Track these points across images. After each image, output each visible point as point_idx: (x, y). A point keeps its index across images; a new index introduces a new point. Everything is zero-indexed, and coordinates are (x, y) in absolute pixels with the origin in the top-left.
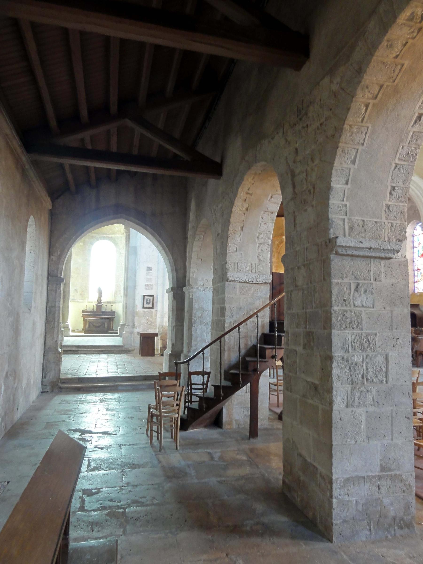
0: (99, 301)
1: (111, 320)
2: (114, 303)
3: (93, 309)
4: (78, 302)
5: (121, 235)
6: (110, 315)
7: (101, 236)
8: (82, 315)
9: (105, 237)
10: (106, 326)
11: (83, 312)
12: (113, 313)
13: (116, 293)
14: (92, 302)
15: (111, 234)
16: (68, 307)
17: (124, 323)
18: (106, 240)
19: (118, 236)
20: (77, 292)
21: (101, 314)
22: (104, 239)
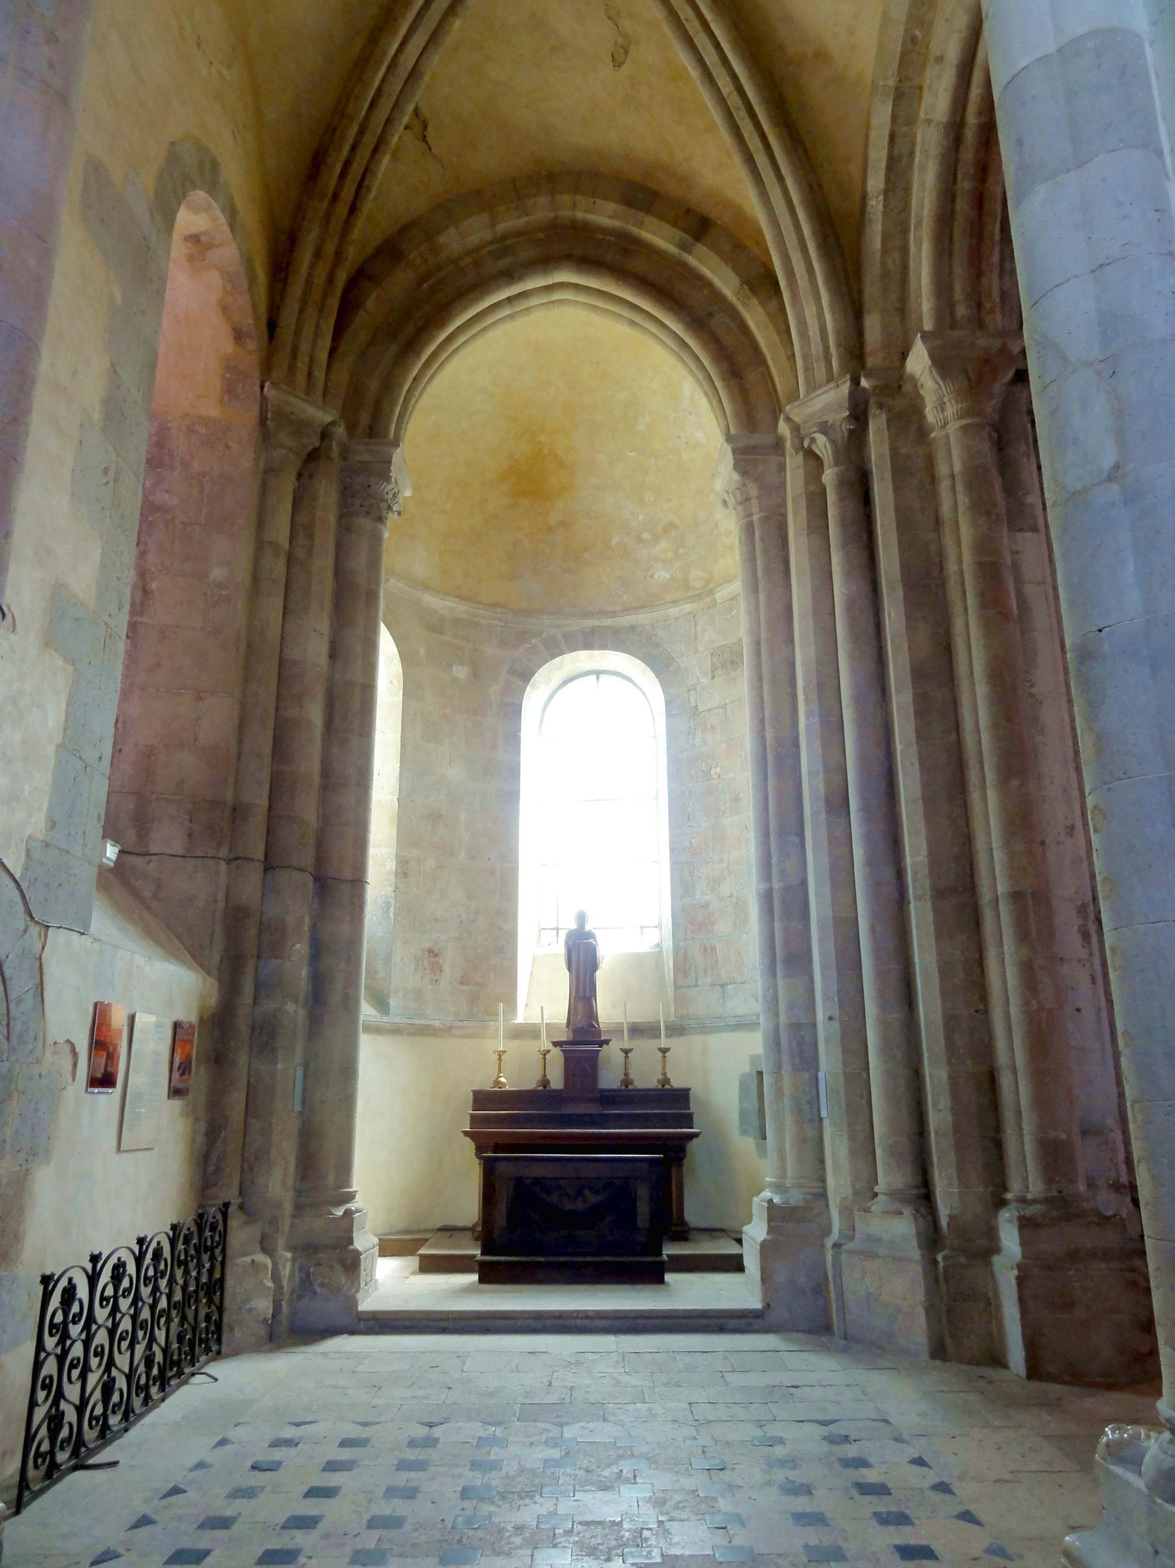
1: (674, 1152)
2: (676, 1030)
3: (545, 1082)
4: (448, 1030)
5: (688, 607)
6: (663, 1121)
7: (575, 625)
8: (474, 1120)
9: (593, 630)
10: (643, 1209)
11: (482, 1099)
12: (674, 1103)
13: (683, 966)
14: (530, 1032)
15: (628, 610)
16: (348, 1072)
17: (796, 1198)
18: (603, 647)
19: (673, 611)
20: (437, 969)
21: (594, 1109)
22: (588, 646)
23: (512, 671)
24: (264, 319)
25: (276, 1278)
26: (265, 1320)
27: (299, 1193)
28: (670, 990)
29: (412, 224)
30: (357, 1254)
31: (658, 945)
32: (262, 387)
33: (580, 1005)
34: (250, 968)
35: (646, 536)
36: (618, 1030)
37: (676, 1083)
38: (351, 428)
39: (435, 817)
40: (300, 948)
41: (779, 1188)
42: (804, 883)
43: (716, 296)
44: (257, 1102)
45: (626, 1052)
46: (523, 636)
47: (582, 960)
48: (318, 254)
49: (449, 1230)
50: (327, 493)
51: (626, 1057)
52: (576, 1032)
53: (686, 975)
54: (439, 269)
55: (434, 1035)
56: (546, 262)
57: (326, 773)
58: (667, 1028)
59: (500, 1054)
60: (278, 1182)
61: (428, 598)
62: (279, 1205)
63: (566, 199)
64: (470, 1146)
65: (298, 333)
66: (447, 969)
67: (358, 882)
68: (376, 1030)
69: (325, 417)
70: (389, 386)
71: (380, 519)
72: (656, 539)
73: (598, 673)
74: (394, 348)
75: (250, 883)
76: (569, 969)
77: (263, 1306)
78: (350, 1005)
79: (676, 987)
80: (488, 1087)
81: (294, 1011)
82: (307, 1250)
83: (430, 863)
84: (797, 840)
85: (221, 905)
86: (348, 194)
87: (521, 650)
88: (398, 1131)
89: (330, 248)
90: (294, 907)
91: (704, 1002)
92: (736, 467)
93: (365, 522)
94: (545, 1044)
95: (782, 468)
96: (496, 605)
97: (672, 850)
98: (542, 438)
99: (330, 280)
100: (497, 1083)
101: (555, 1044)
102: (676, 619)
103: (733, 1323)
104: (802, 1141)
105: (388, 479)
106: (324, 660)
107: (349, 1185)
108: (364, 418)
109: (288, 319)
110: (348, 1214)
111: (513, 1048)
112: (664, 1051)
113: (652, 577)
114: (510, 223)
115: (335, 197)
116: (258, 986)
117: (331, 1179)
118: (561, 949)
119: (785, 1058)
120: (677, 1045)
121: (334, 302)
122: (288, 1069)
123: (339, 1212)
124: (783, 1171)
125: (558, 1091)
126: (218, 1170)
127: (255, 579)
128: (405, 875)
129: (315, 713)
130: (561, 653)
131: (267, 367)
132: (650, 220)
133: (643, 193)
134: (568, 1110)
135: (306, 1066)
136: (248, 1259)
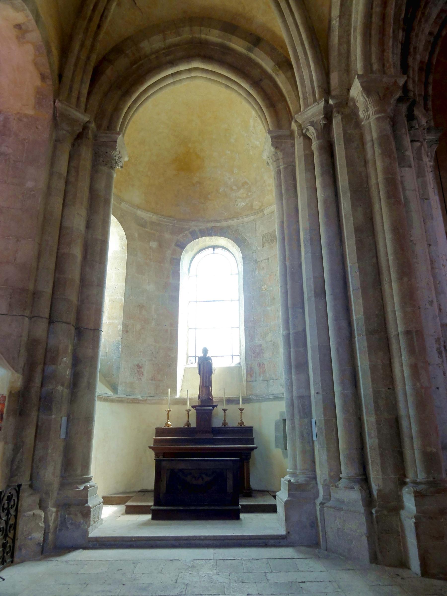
0: (204, 397)
1: (245, 456)
2: (246, 401)
3: (188, 424)
5: (252, 217)
8: (156, 442)
9: (212, 228)
10: (230, 483)
11: (160, 432)
12: (246, 433)
13: (250, 371)
14: (182, 402)
16: (89, 420)
17: (301, 479)
18: (216, 235)
19: (246, 219)
21: (210, 436)
23: (177, 245)
24: (56, 72)
25: (46, 521)
26: (39, 544)
27: (62, 477)
28: (245, 383)
29: (128, 38)
30: (89, 508)
31: (239, 364)
32: (54, 102)
33: (204, 390)
34: (39, 369)
35: (234, 188)
36: (221, 401)
37: (247, 424)
38: (99, 127)
39: (141, 307)
40: (66, 361)
41: (294, 474)
42: (304, 330)
43: (264, 72)
44: (40, 433)
45: (225, 410)
46: (181, 230)
47: (205, 369)
48: (82, 45)
49: (144, 492)
50: (86, 154)
51: (225, 413)
52: (202, 401)
53: (251, 376)
54: (140, 59)
55: (138, 403)
56: (188, 58)
57: (83, 279)
58: (243, 400)
59: (169, 412)
60: (51, 473)
61: (139, 213)
62: (51, 484)
63: (197, 28)
64: (153, 453)
65: (72, 81)
66: (145, 374)
67: (97, 330)
68: (105, 399)
69: (85, 118)
70: (117, 109)
71: (112, 168)
72: (239, 189)
73: (214, 247)
74: (120, 93)
75: (41, 329)
76: (200, 373)
77: (38, 536)
78: (91, 387)
79: (247, 382)
80: (162, 425)
81: (62, 390)
82: (64, 506)
83: (138, 327)
84: (301, 310)
85: (25, 339)
86: (96, 19)
87: (181, 235)
88: (115, 447)
89: (88, 43)
90: (64, 340)
91: (260, 388)
92: (272, 145)
93: (104, 169)
94: (189, 407)
95: (293, 146)
96: (170, 217)
97: (245, 321)
98: (190, 145)
99: (88, 58)
100: (167, 424)
101: (193, 407)
102: (247, 223)
103: (272, 542)
104: (304, 452)
105: (115, 149)
106: (82, 228)
107: (88, 473)
108: (105, 123)
109: (68, 74)
110: (86, 488)
111: (175, 409)
112: (242, 410)
113: (237, 205)
114: (172, 40)
115: (90, 20)
116: (43, 378)
117: (79, 471)
118: (196, 365)
119: (296, 412)
120: (246, 407)
121: (90, 69)
122: (59, 419)
123: (82, 487)
124: (295, 466)
125: (194, 428)
126: (18, 467)
127: (49, 188)
128: (127, 331)
129: (77, 251)
130: (199, 238)
131: (57, 94)
132: (235, 38)
133: (231, 26)
134: (197, 437)
135: (68, 416)
136: (31, 513)
